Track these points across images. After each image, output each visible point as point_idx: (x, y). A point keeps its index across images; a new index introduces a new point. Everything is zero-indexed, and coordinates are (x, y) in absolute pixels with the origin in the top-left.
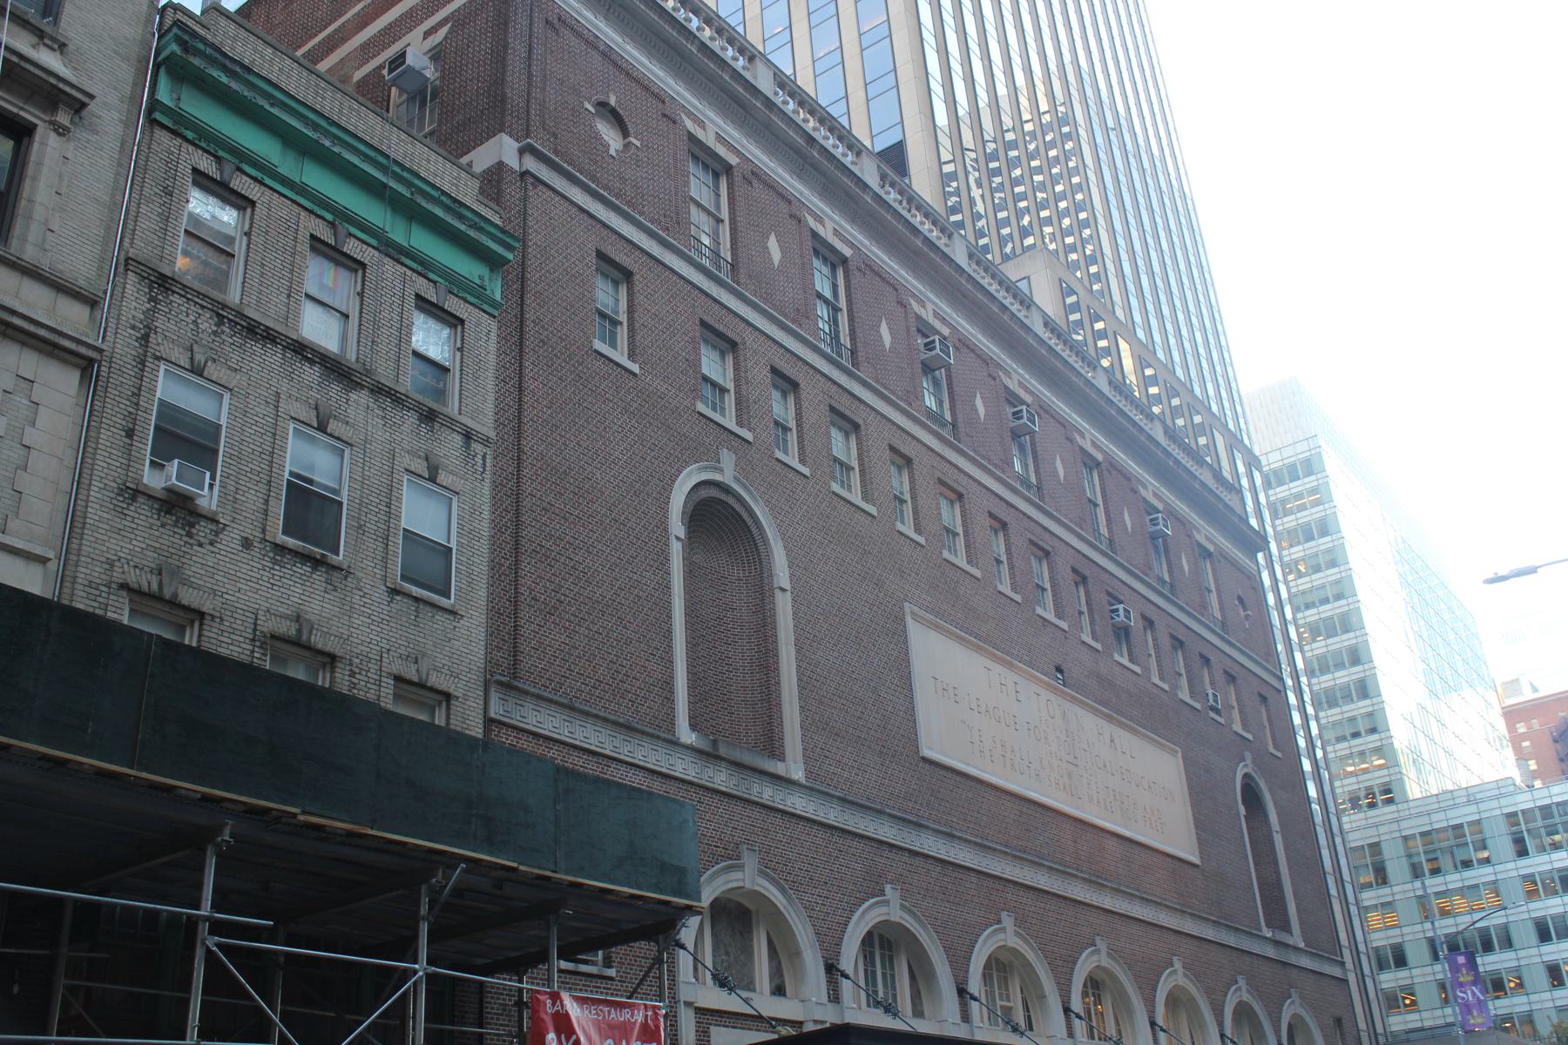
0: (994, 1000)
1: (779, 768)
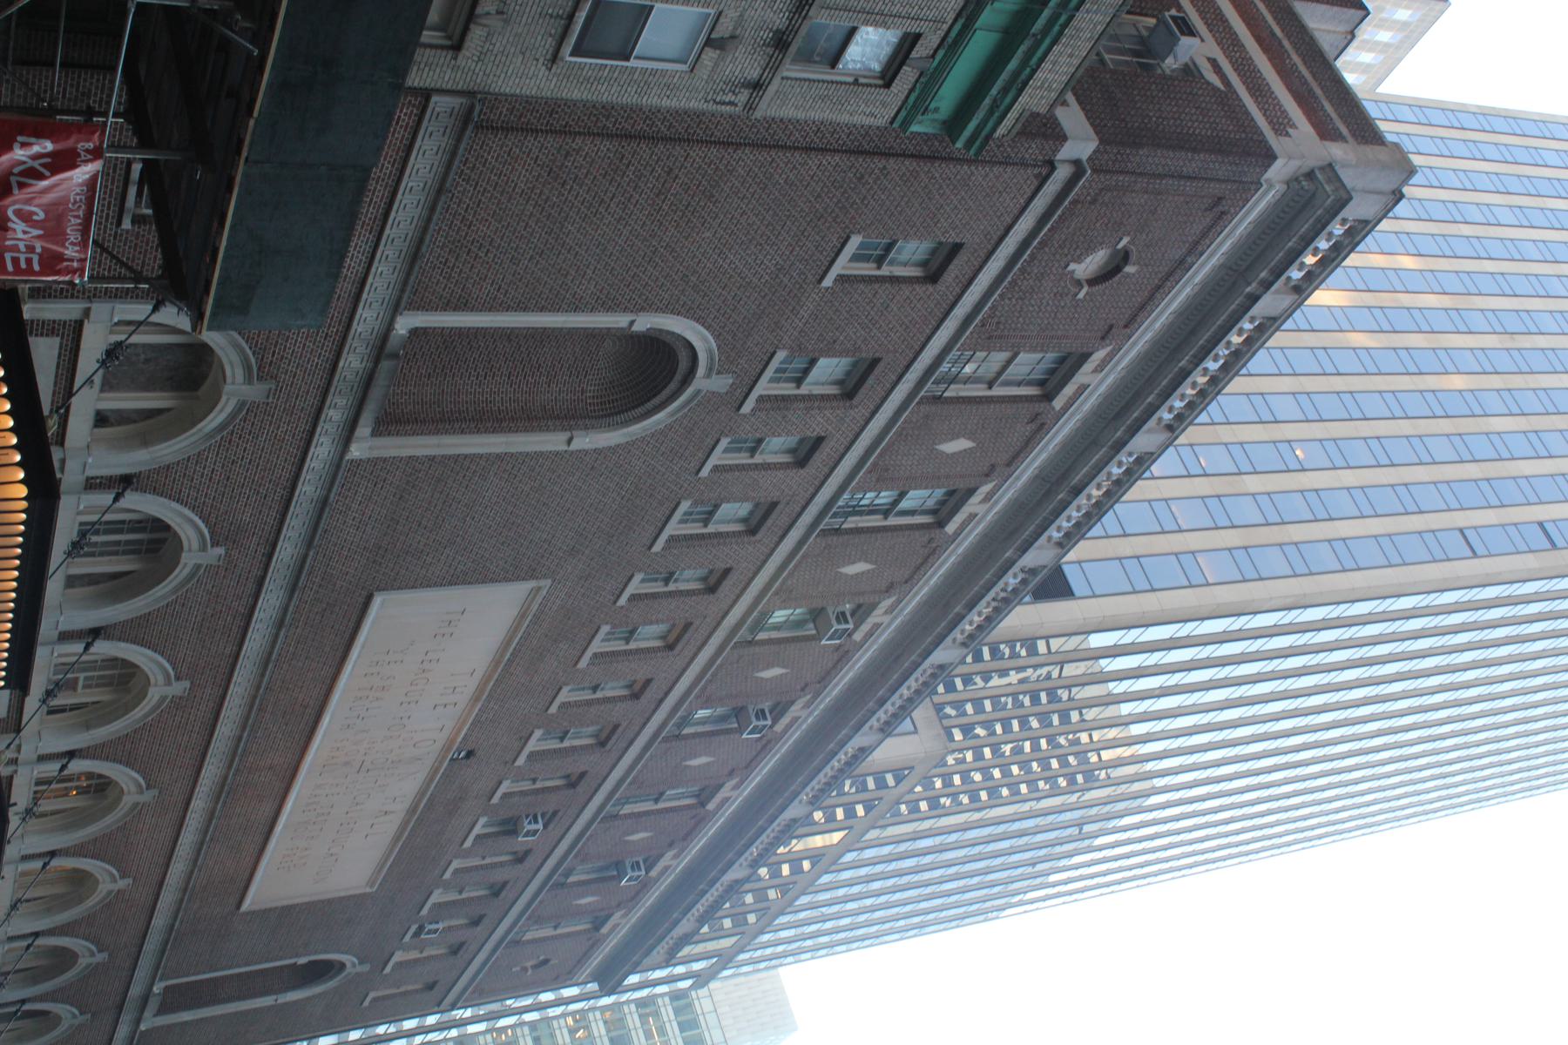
0: (84, 670)
1: (364, 430)
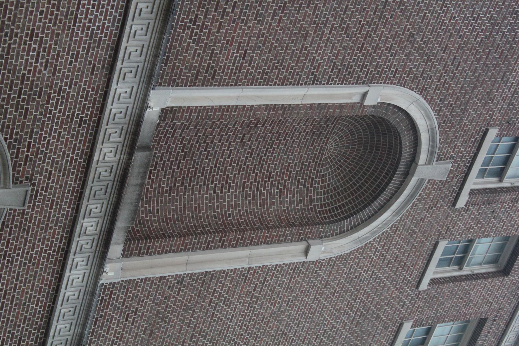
1: (116, 249)
